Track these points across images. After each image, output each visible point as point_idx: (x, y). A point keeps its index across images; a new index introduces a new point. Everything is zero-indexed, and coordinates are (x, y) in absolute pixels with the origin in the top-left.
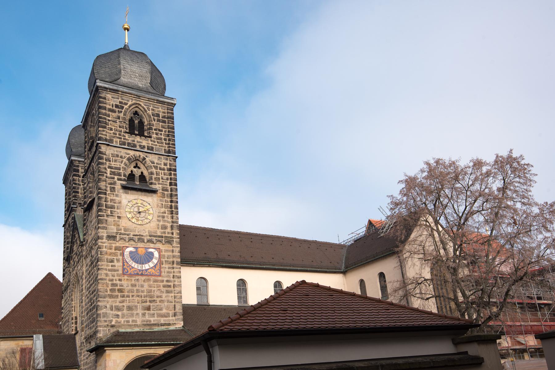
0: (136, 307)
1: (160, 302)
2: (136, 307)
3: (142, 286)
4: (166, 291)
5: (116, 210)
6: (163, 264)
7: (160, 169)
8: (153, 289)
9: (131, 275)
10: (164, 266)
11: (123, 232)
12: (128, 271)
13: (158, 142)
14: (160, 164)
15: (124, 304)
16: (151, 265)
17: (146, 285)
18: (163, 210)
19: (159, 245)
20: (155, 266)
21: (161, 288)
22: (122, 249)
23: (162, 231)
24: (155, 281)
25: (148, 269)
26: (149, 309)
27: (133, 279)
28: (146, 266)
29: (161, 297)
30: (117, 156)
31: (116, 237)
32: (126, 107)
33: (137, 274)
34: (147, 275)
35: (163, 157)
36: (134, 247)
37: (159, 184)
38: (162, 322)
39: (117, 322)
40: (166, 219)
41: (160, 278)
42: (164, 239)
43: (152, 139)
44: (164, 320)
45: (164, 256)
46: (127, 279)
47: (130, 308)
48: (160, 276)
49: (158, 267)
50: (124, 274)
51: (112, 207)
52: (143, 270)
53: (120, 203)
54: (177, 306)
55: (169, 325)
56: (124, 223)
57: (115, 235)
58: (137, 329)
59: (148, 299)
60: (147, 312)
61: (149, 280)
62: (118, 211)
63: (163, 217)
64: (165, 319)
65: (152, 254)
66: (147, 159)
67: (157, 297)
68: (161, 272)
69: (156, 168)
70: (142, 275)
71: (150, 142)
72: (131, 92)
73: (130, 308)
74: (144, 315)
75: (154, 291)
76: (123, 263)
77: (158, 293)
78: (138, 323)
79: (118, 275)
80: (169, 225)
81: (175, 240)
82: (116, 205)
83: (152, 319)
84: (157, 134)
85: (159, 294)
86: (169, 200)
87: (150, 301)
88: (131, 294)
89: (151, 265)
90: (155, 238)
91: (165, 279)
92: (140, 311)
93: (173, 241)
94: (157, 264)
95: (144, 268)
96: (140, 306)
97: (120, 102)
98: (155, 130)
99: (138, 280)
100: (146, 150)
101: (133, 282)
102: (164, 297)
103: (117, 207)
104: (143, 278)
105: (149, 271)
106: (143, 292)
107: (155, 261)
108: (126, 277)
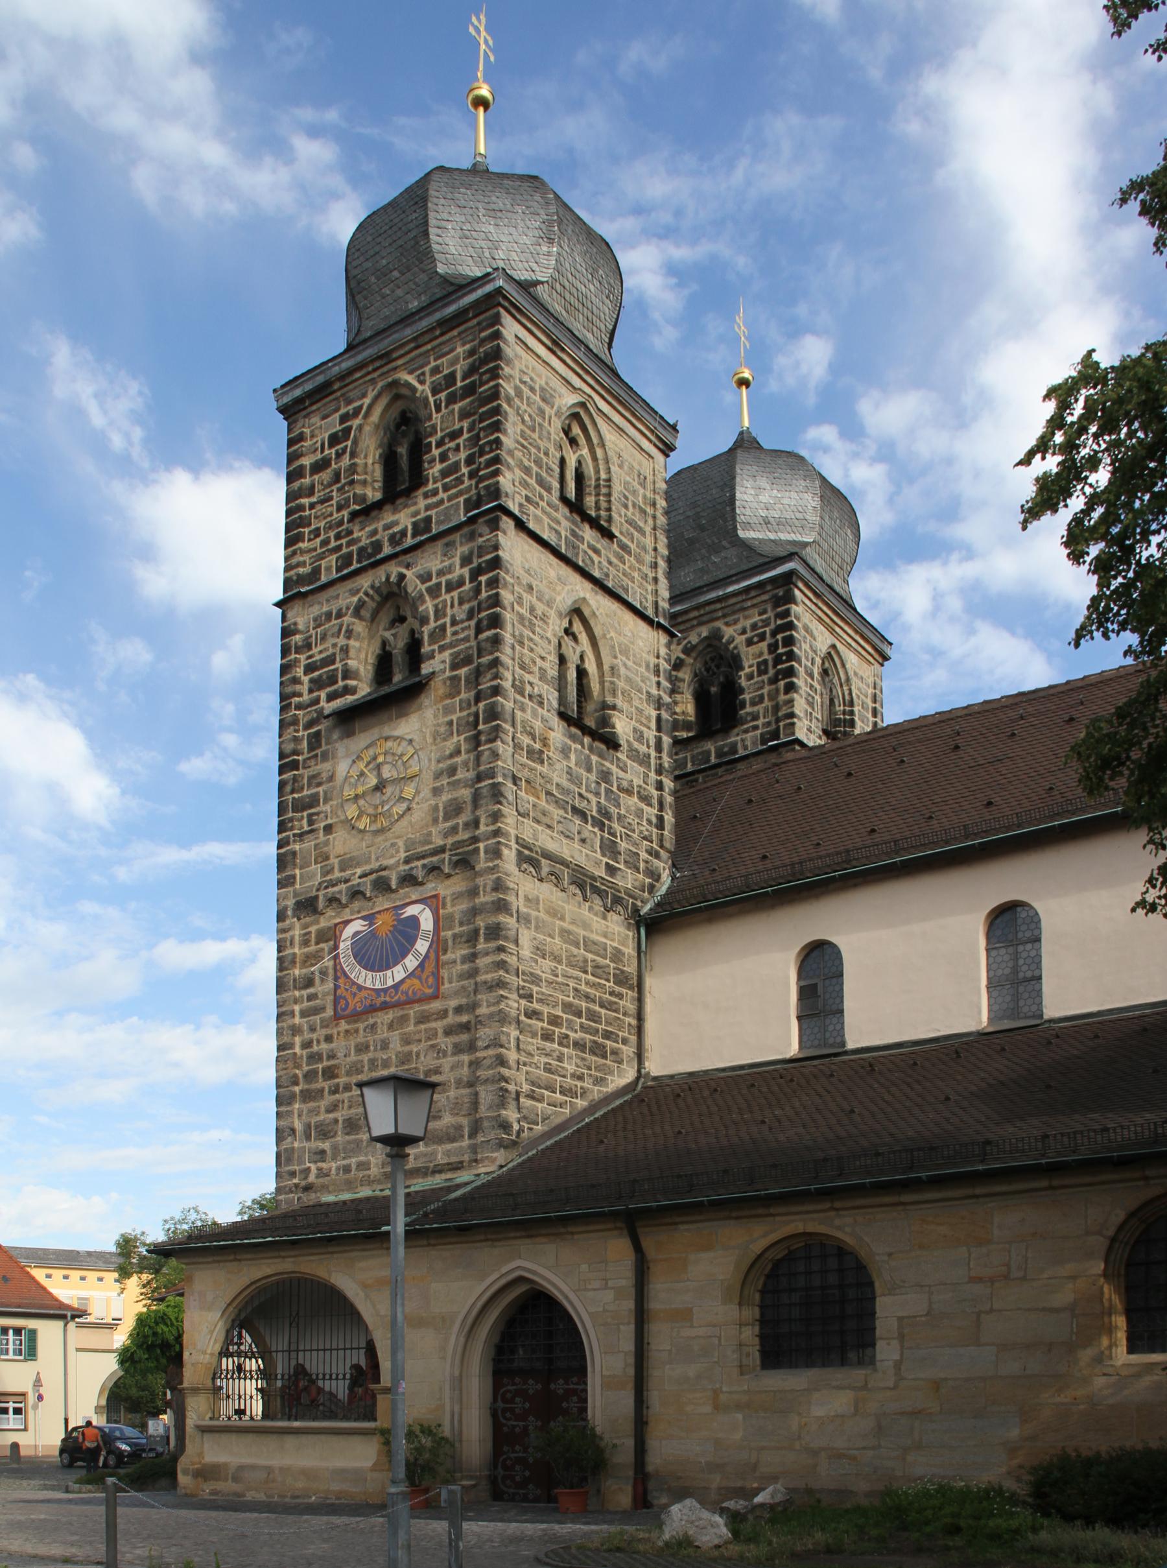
3: (385, 1045)
4: (456, 1046)
5: (322, 808)
6: (445, 951)
7: (450, 587)
8: (415, 1048)
9: (355, 1016)
10: (449, 956)
11: (337, 874)
12: (347, 1004)
13: (446, 488)
14: (450, 569)
16: (411, 962)
17: (395, 1037)
18: (450, 745)
20: (421, 965)
22: (331, 936)
23: (448, 824)
24: (423, 1018)
25: (402, 981)
27: (361, 1026)
28: (397, 973)
30: (329, 616)
31: (317, 897)
33: (372, 1009)
34: (398, 1005)
35: (457, 537)
36: (363, 918)
37: (442, 649)
38: (441, 1159)
41: (436, 1005)
42: (446, 856)
43: (431, 486)
44: (448, 1153)
45: (451, 917)
46: (347, 1031)
48: (435, 997)
49: (430, 967)
50: (337, 1017)
51: (314, 801)
52: (385, 990)
53: (331, 778)
54: (482, 1095)
55: (457, 1167)
56: (341, 843)
57: (314, 893)
61: (403, 1019)
62: (327, 808)
63: (452, 771)
64: (449, 1146)
65: (414, 921)
66: (409, 574)
68: (439, 980)
69: (434, 592)
70: (385, 1006)
72: (360, 358)
75: (418, 1055)
76: (336, 979)
79: (325, 1024)
80: (466, 793)
81: (481, 845)
82: (320, 789)
89: (411, 962)
90: (419, 863)
91: (453, 1003)
93: (477, 850)
94: (427, 956)
95: (390, 983)
98: (440, 444)
99: (373, 1027)
100: (409, 541)
101: (360, 1039)
102: (446, 1068)
103: (325, 793)
105: (404, 987)
107: (422, 946)
108: (343, 1025)
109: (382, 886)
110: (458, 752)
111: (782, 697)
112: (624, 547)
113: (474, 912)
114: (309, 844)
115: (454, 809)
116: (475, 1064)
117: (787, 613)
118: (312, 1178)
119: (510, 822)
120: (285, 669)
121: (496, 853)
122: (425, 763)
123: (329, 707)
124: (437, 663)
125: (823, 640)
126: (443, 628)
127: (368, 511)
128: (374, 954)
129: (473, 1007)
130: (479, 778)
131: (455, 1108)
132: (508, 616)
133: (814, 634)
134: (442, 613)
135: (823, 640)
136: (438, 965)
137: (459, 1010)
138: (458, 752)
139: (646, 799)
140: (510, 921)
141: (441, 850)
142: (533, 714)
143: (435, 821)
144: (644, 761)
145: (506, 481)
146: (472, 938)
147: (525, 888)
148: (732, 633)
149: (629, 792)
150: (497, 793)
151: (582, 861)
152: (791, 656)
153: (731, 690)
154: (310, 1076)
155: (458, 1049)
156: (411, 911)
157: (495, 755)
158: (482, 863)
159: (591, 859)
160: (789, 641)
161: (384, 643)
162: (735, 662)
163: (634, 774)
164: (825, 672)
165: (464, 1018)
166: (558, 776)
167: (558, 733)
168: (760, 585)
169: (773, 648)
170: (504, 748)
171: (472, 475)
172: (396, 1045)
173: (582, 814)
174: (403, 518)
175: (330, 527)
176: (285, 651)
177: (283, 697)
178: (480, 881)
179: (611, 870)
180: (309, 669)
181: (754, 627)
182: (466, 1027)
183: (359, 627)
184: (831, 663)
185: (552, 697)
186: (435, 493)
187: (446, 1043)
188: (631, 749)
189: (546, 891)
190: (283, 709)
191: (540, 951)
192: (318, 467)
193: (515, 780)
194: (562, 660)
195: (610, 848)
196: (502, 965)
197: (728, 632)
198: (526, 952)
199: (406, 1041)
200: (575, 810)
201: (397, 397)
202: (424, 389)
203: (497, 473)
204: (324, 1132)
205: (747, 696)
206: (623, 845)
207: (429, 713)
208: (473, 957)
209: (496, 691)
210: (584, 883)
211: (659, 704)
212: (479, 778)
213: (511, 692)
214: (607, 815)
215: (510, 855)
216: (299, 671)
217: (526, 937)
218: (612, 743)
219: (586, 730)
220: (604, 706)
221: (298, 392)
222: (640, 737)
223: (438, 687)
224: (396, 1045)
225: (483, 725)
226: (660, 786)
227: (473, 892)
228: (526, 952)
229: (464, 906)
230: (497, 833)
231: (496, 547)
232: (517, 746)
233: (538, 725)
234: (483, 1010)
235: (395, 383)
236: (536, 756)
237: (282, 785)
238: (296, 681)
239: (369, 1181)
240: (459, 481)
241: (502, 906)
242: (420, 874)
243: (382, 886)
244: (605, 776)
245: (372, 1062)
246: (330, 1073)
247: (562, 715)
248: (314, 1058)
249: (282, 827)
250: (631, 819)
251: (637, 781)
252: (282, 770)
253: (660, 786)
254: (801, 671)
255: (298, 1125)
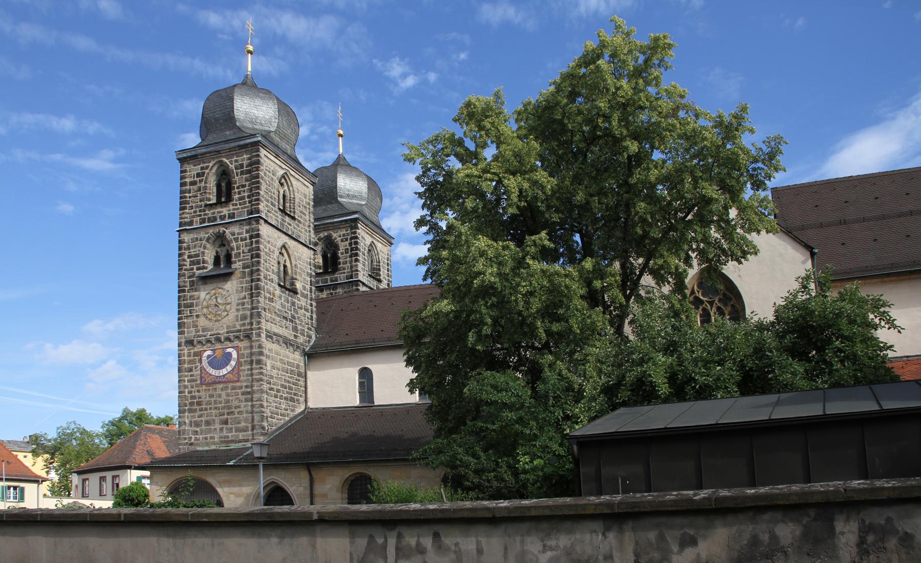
0: (214, 420)
1: (238, 413)
2: (214, 420)
3: (220, 396)
7: (242, 240)
14: (242, 233)
15: (203, 419)
16: (229, 368)
17: (223, 393)
19: (236, 343)
21: (240, 396)
24: (234, 388)
26: (226, 422)
28: (224, 371)
29: (239, 407)
32: (207, 171)
33: (215, 383)
37: (239, 261)
39: (196, 439)
40: (246, 306)
41: (238, 384)
47: (208, 423)
48: (238, 381)
49: (236, 371)
58: (213, 447)
59: (226, 411)
60: (225, 426)
61: (227, 388)
63: (243, 304)
65: (230, 354)
67: (236, 408)
68: (239, 376)
69: (236, 240)
70: (220, 382)
71: (231, 207)
73: (208, 423)
74: (221, 429)
77: (236, 403)
78: (216, 440)
80: (249, 313)
83: (230, 434)
84: (239, 193)
85: (238, 404)
86: (249, 279)
87: (228, 414)
88: (208, 407)
89: (229, 368)
91: (245, 384)
92: (218, 426)
96: (217, 419)
97: (202, 168)
98: (238, 188)
101: (211, 392)
104: (221, 386)
106: (220, 403)
107: (233, 363)
109: (218, 340)
110: (245, 298)
111: (354, 263)
112: (299, 222)
113: (252, 354)
114: (190, 320)
115: (244, 317)
116: (252, 406)
117: (355, 233)
118: (193, 440)
119: (264, 325)
120: (180, 255)
121: (259, 335)
122: (234, 299)
123: (198, 273)
124: (237, 265)
125: (369, 240)
126: (239, 253)
127: (211, 206)
128: (217, 363)
129: (252, 386)
130: (253, 308)
131: (246, 420)
132: (262, 254)
133: (365, 237)
134: (239, 248)
135: (369, 240)
136: (239, 371)
137: (246, 387)
138: (245, 298)
139: (307, 310)
140: (264, 358)
141: (240, 331)
142: (270, 285)
143: (237, 320)
144: (306, 296)
145: (261, 207)
146: (251, 362)
147: (268, 345)
148: (336, 235)
149: (301, 308)
150: (259, 315)
151: (286, 335)
152: (357, 249)
153: (335, 257)
154: (192, 404)
155: (246, 400)
156: (229, 350)
157: (258, 302)
158: (254, 338)
159: (288, 333)
160: (356, 243)
161: (217, 252)
162: (337, 247)
163: (303, 302)
164: (369, 250)
165: (249, 390)
166: (278, 307)
167: (278, 291)
168: (346, 221)
169: (350, 244)
170: (261, 299)
171: (250, 202)
172: (224, 396)
173: (285, 318)
174: (225, 211)
175: (197, 207)
176: (180, 248)
177: (179, 265)
178: (253, 344)
179: (296, 337)
180: (189, 257)
181: (344, 235)
182: (248, 393)
183: (208, 246)
184: (372, 247)
185: (276, 278)
186: (236, 205)
187: (242, 398)
188: (302, 293)
189: (275, 346)
190: (179, 270)
191: (273, 367)
192: (193, 183)
193: (265, 309)
194: (279, 263)
195: (295, 329)
196: (261, 373)
197: (335, 235)
198: (269, 368)
199: (228, 395)
200: (284, 317)
201: (222, 165)
202: (232, 166)
203: (258, 204)
204: (197, 424)
205: (341, 260)
206: (299, 327)
207: (235, 282)
208: (252, 369)
209: (259, 280)
210: (287, 342)
211: (311, 276)
212: (253, 308)
213: (264, 280)
214: (294, 318)
215: (263, 335)
216: (186, 257)
217: (269, 363)
218: (295, 292)
219: (287, 289)
220: (293, 278)
221: (185, 155)
222: (304, 288)
223: (238, 274)
224: (224, 396)
225: (254, 290)
226: (311, 305)
227: (251, 347)
228: (269, 368)
229: (249, 351)
230: (259, 328)
231: (258, 230)
232: (265, 298)
233: (272, 289)
234: (255, 388)
235: (222, 161)
236: (271, 300)
237: (179, 297)
238: (184, 260)
239: (214, 443)
240: (245, 203)
241: (261, 353)
242: (232, 338)
243: (218, 340)
244: (293, 304)
245: (215, 401)
246: (199, 403)
247: (279, 285)
248: (193, 397)
249: (179, 312)
250: (302, 318)
251: (304, 304)
252: (179, 292)
253: (311, 305)
254: (361, 254)
255: (187, 421)
